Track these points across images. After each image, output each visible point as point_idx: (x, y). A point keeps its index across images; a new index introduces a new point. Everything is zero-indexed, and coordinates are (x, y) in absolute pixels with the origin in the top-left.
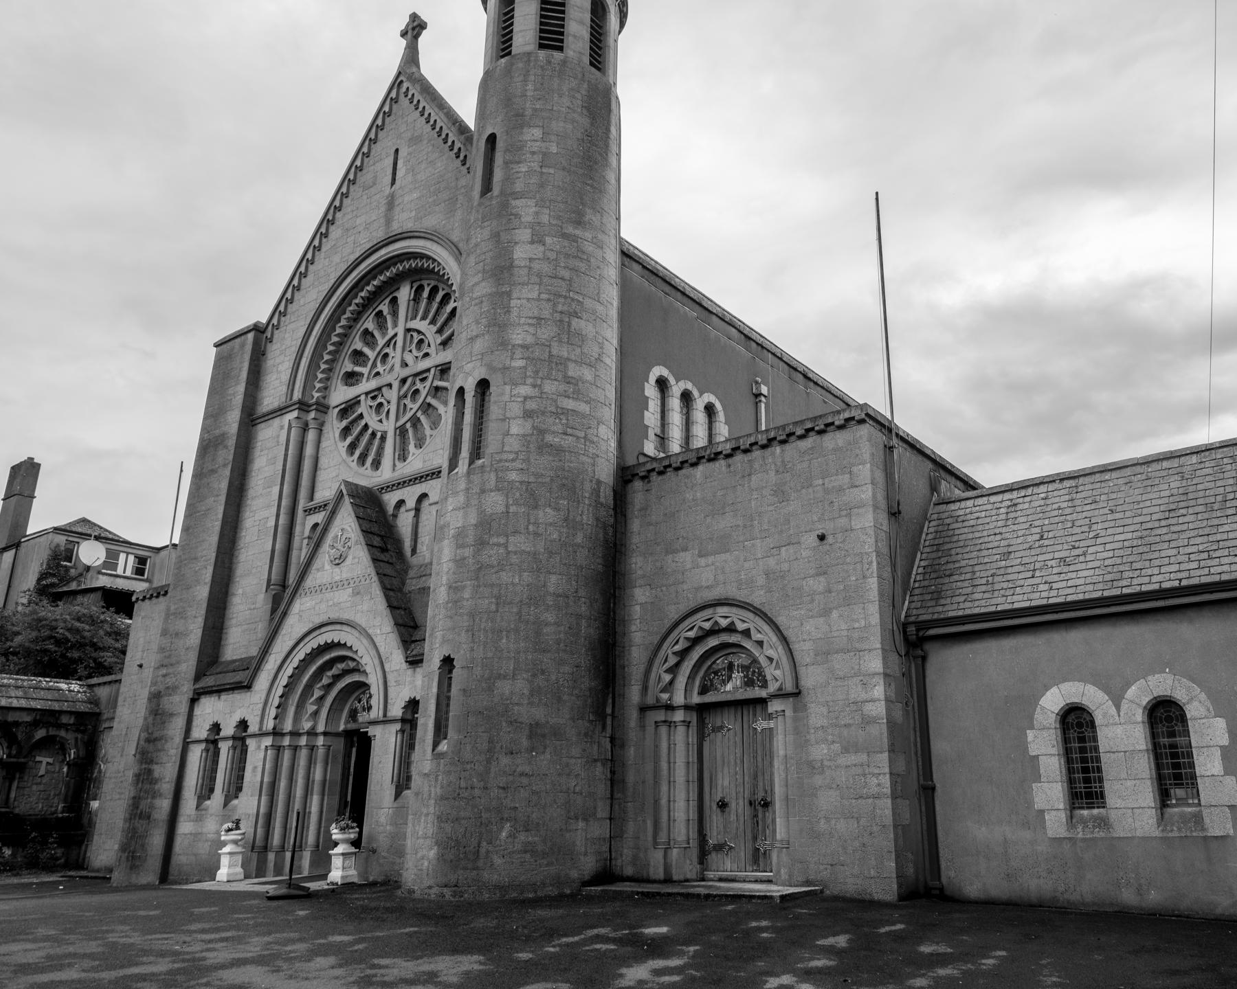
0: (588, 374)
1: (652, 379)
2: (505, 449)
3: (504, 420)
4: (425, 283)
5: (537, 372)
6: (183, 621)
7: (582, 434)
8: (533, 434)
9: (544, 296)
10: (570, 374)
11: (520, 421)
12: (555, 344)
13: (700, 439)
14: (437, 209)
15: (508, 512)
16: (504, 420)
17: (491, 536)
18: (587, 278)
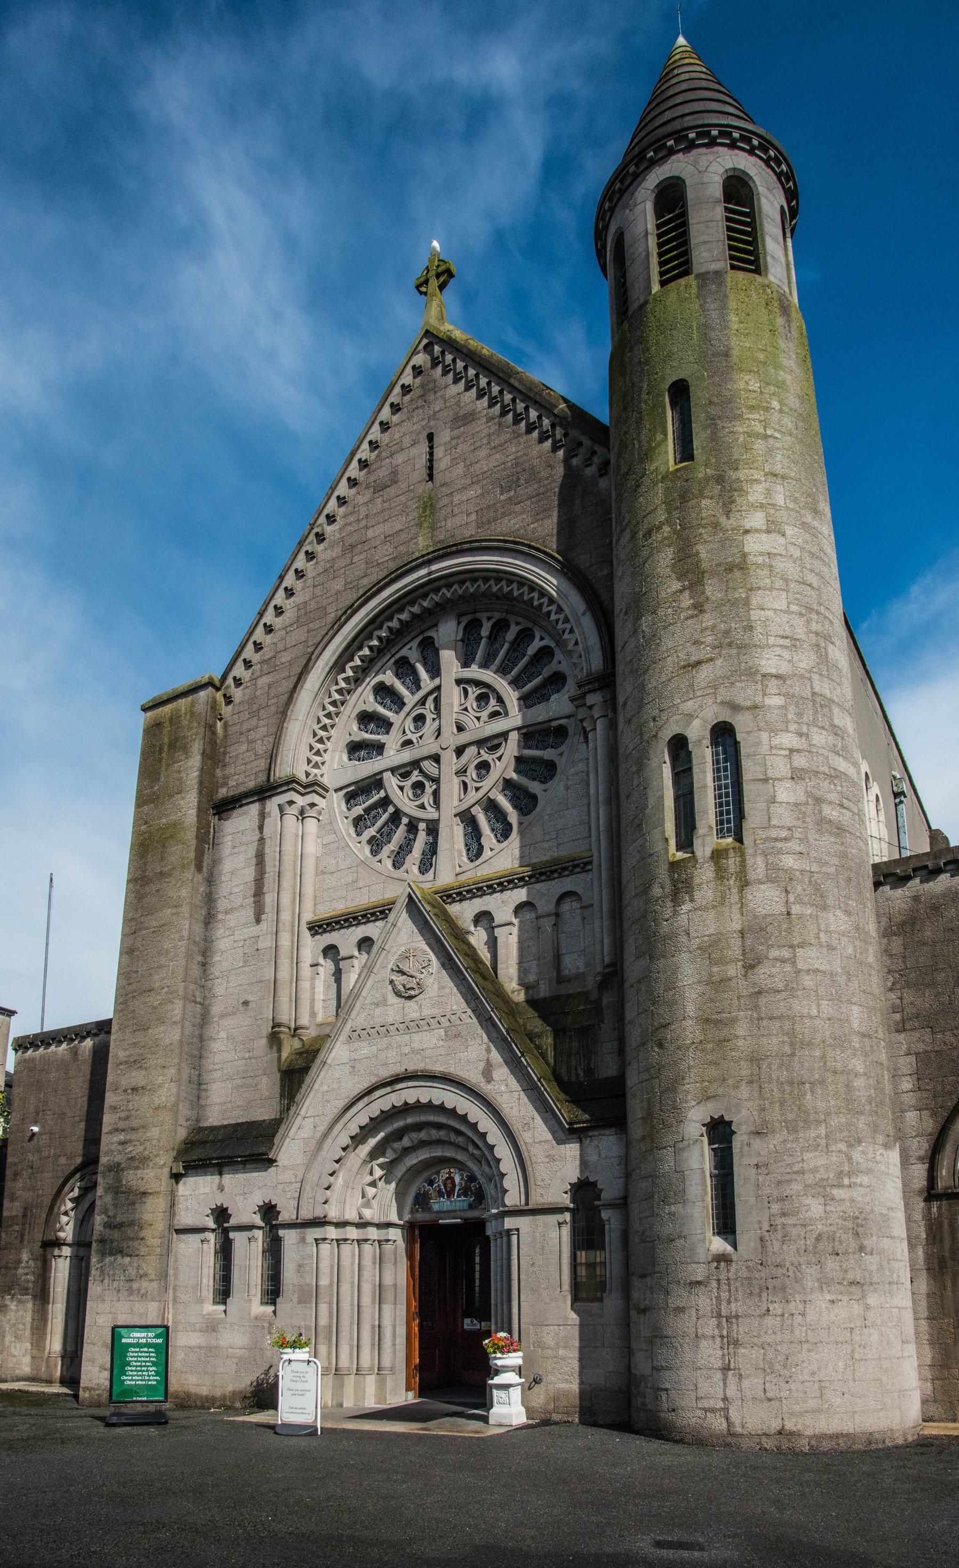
2: (772, 823)
3: (766, 780)
5: (800, 715)
8: (807, 804)
11: (789, 784)
15: (788, 914)
16: (766, 780)
17: (770, 947)
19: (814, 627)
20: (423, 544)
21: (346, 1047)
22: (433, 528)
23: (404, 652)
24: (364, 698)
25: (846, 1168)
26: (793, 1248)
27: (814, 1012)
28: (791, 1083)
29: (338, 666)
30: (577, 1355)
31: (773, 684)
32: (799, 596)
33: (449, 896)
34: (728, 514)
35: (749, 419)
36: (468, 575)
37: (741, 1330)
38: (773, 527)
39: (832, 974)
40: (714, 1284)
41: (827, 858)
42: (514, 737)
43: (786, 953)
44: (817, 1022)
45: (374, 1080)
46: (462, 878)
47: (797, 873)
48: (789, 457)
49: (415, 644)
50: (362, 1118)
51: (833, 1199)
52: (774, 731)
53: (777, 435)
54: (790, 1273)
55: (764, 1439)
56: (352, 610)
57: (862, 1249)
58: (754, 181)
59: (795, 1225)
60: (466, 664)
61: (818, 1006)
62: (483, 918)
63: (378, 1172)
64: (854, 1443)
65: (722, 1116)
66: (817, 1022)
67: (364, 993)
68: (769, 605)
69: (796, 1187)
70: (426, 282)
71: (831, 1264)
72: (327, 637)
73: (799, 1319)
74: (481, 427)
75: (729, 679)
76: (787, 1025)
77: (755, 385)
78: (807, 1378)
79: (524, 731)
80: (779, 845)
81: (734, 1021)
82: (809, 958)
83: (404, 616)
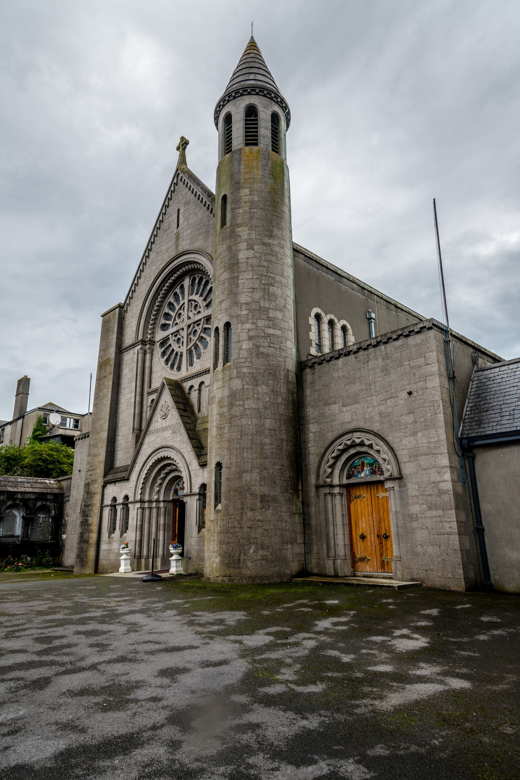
8: (253, 348)
11: (247, 342)
15: (243, 389)
17: (236, 401)
19: (263, 282)
39: (258, 409)
43: (241, 403)
49: (179, 287)
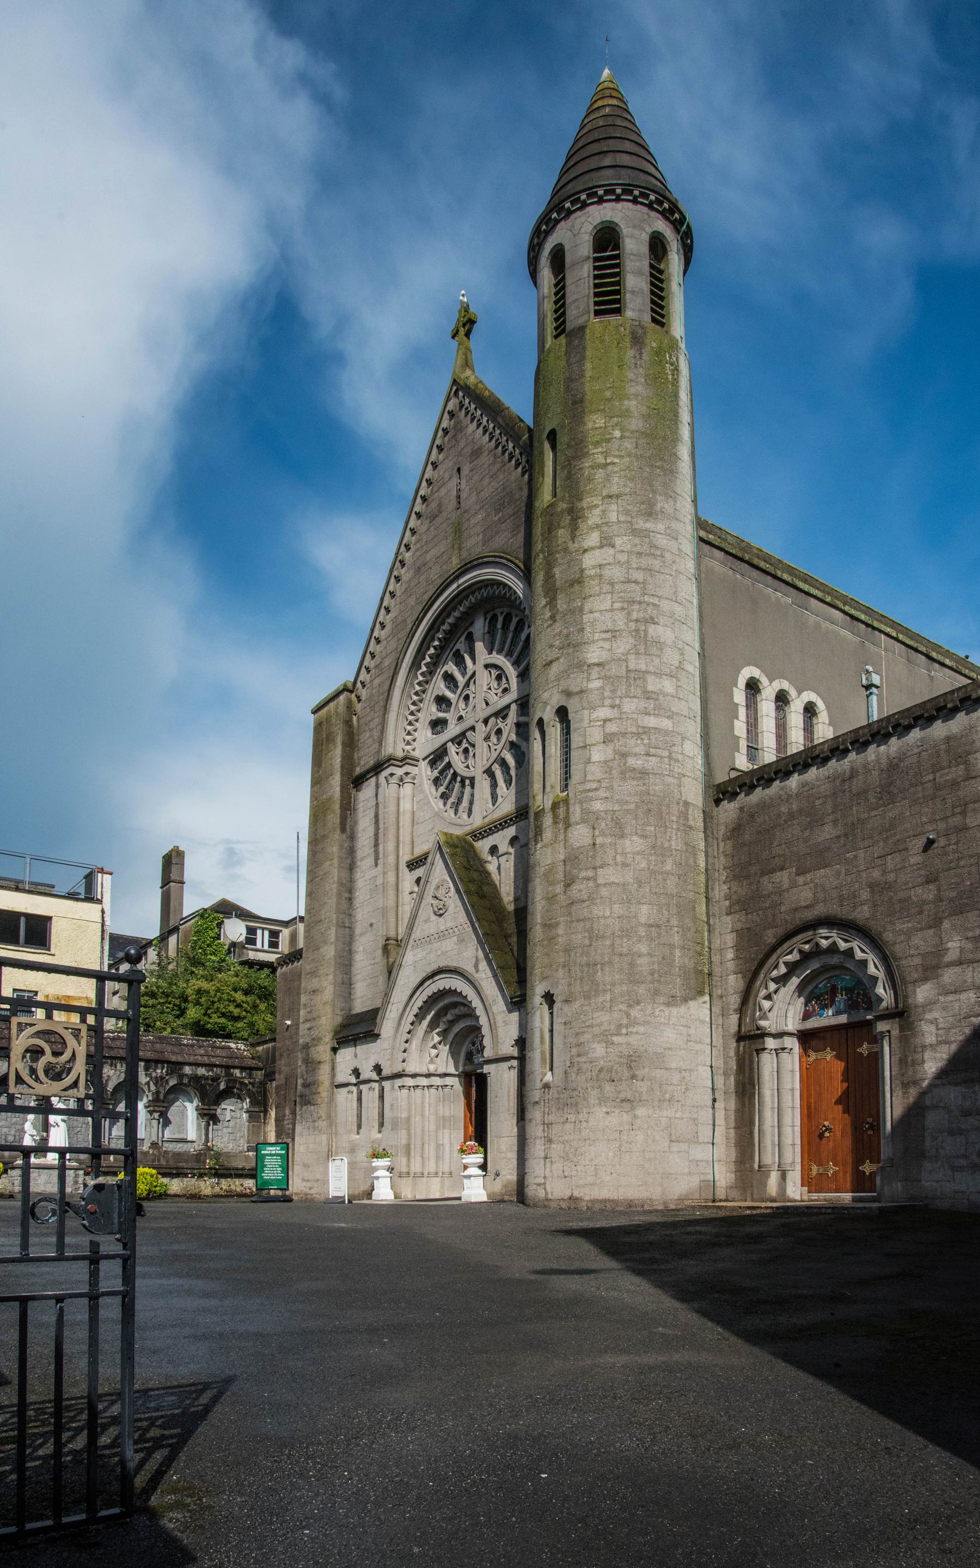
0: (668, 686)
1: (742, 683)
3: (585, 747)
4: (498, 611)
5: (614, 691)
6: (318, 979)
7: (666, 753)
8: (614, 759)
9: (617, 605)
10: (650, 688)
11: (601, 747)
12: (631, 657)
13: (796, 741)
14: (503, 526)
15: (594, 844)
16: (585, 747)
18: (662, 577)
19: (634, 615)
20: (455, 563)
21: (411, 953)
22: (460, 549)
23: (458, 646)
24: (439, 686)
25: (625, 1022)
26: (583, 1077)
27: (608, 913)
28: (588, 965)
29: (415, 665)
30: (516, 1156)
31: (595, 672)
32: (622, 594)
33: (475, 836)
34: (573, 538)
35: (593, 454)
36: (468, 591)
37: (555, 1130)
38: (607, 542)
39: (624, 884)
40: (542, 1103)
41: (628, 799)
42: (514, 707)
43: (590, 873)
44: (609, 921)
45: (424, 975)
46: (487, 820)
47: (603, 814)
48: (625, 476)
49: (463, 639)
50: (419, 1001)
51: (613, 1043)
52: (593, 708)
53: (616, 460)
54: (581, 1095)
55: (562, 1202)
56: (419, 621)
57: (633, 1077)
58: (619, 227)
59: (585, 1062)
60: (490, 653)
61: (611, 908)
62: (494, 850)
63: (437, 1039)
64: (617, 1206)
65: (549, 991)
66: (609, 921)
67: (419, 914)
68: (597, 608)
69: (587, 1037)
70: (457, 332)
71: (608, 1088)
72: (406, 644)
73: (584, 1124)
74: (485, 459)
75: (566, 674)
76: (588, 926)
77: (600, 422)
78: (587, 1163)
79: (519, 702)
80: (590, 794)
81: (557, 924)
82: (608, 875)
83: (451, 620)
